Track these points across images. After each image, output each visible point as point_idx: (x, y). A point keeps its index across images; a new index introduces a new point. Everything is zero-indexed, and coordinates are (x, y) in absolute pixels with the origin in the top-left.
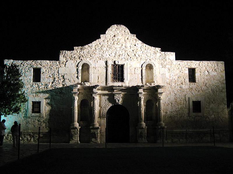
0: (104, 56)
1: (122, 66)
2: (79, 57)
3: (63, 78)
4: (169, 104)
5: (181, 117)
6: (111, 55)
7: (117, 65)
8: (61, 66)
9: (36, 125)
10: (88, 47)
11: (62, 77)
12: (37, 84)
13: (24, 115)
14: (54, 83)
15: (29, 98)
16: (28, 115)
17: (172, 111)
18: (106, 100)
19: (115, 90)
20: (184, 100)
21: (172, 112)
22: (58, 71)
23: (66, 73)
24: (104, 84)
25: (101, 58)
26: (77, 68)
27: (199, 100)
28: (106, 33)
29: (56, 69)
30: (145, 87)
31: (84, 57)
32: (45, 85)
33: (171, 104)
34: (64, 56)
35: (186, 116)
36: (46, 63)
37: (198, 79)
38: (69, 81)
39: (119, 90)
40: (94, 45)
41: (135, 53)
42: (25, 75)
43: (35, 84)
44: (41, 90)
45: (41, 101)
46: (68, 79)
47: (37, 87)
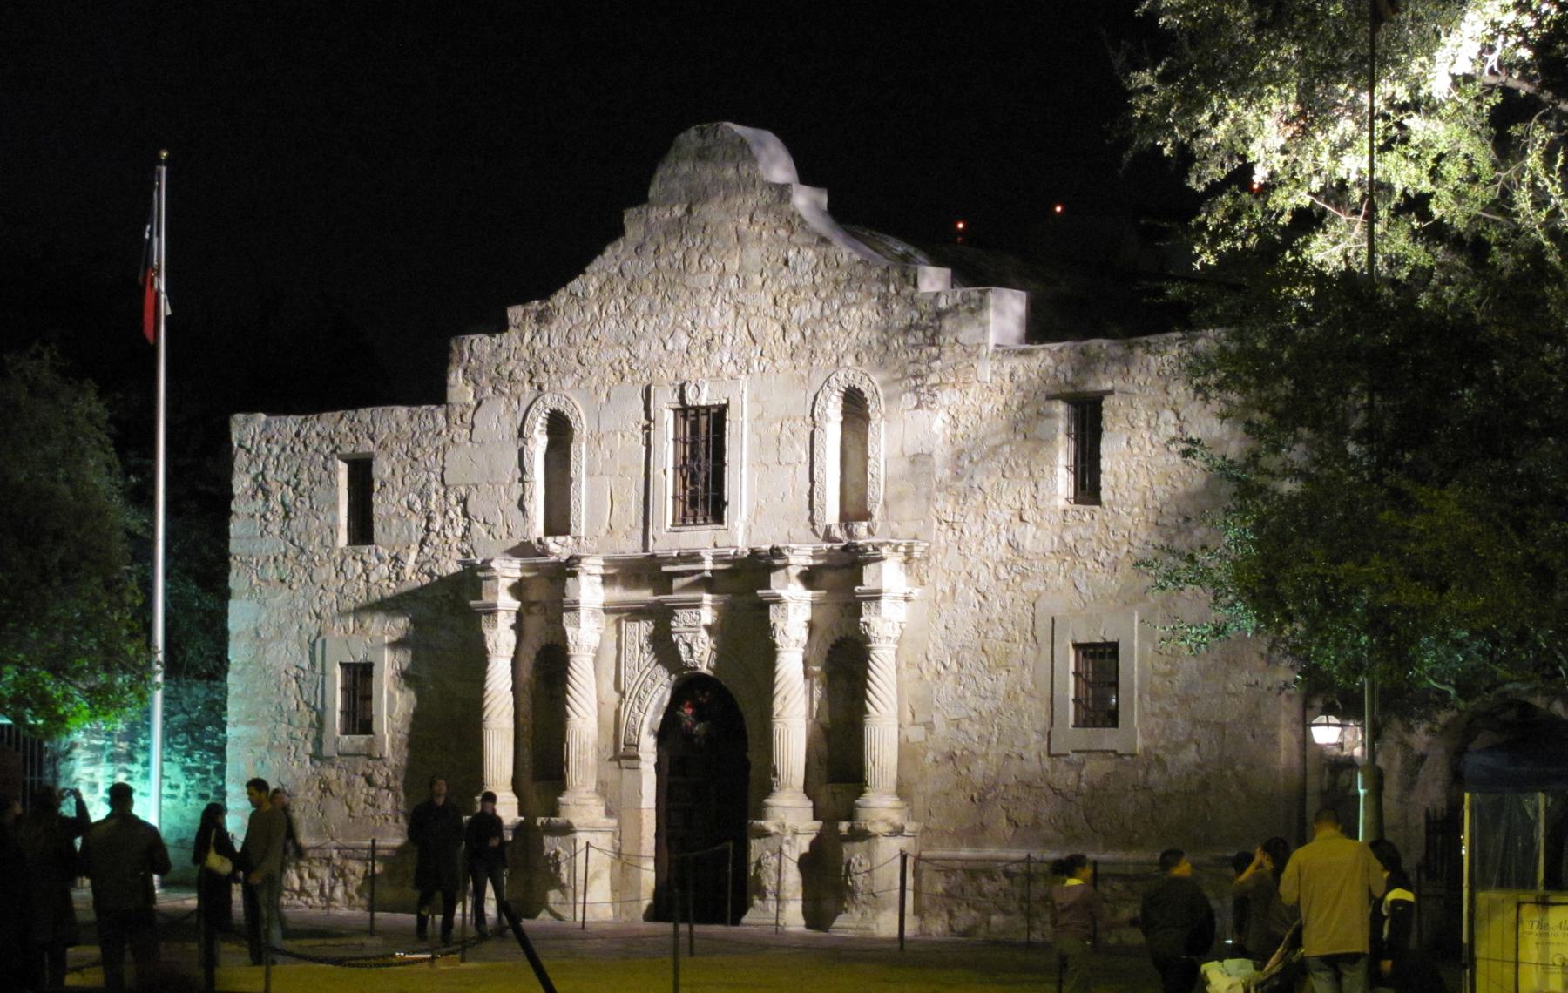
0: (637, 358)
1: (718, 416)
2: (530, 372)
3: (465, 514)
4: (945, 667)
5: (1008, 756)
6: (670, 346)
7: (697, 409)
8: (452, 441)
9: (358, 804)
10: (566, 303)
11: (459, 510)
12: (358, 557)
13: (313, 746)
14: (426, 549)
15: (327, 643)
16: (328, 750)
17: (963, 713)
18: (641, 648)
19: (678, 583)
20: (1029, 636)
21: (957, 723)
22: (443, 468)
23: (476, 481)
24: (631, 547)
25: (626, 368)
26: (521, 444)
27: (1109, 639)
28: (652, 193)
29: (433, 457)
30: (801, 558)
31: (552, 369)
32: (392, 558)
33: (955, 667)
34: (465, 371)
35: (1033, 754)
36: (394, 425)
37: (1112, 482)
38: (489, 532)
39: (687, 580)
40: (597, 285)
41: (784, 315)
42: (312, 507)
43: (354, 558)
44: (376, 595)
45: (373, 660)
46: (485, 522)
47: (359, 576)
